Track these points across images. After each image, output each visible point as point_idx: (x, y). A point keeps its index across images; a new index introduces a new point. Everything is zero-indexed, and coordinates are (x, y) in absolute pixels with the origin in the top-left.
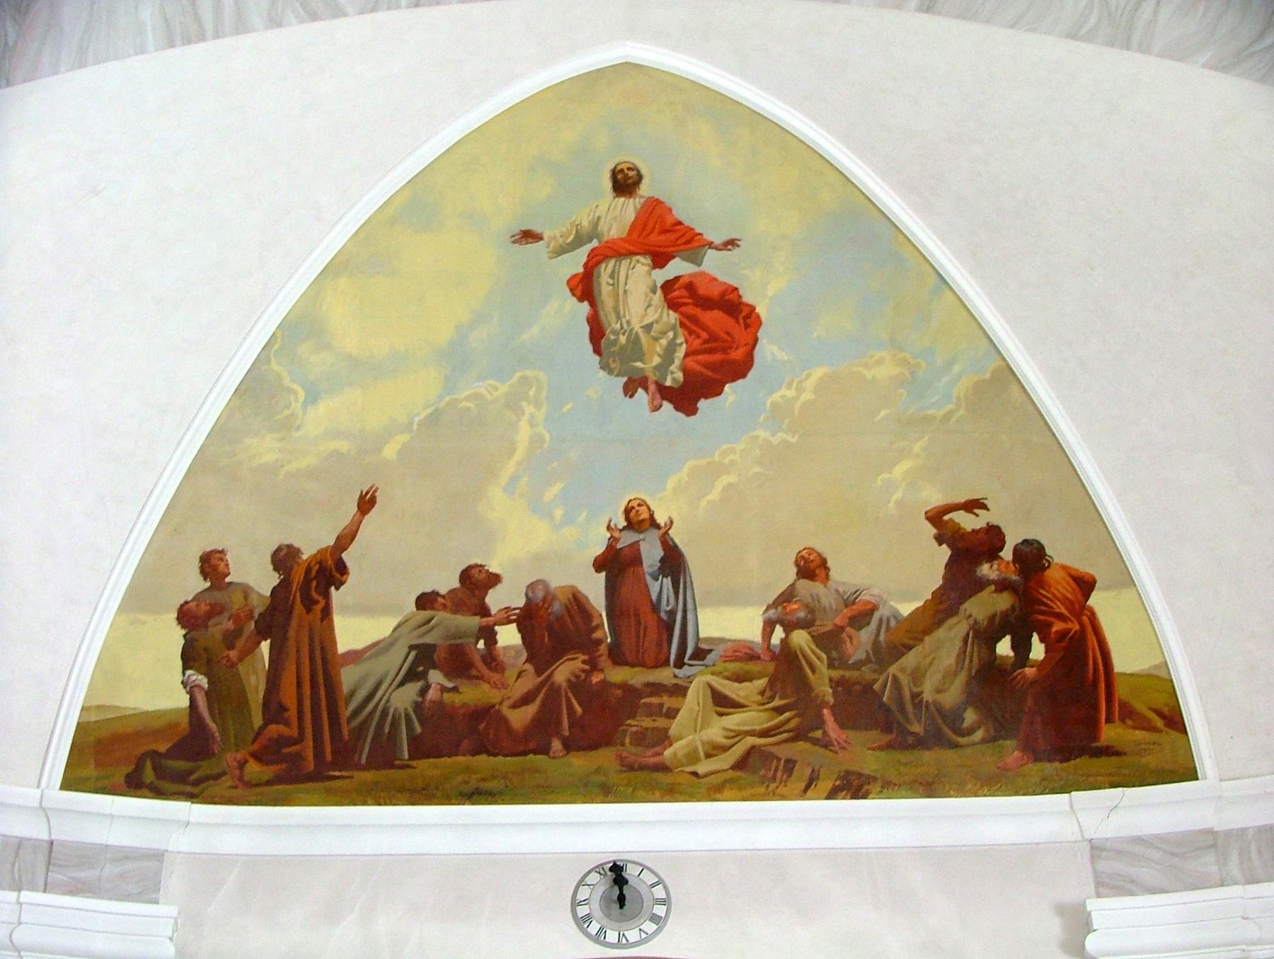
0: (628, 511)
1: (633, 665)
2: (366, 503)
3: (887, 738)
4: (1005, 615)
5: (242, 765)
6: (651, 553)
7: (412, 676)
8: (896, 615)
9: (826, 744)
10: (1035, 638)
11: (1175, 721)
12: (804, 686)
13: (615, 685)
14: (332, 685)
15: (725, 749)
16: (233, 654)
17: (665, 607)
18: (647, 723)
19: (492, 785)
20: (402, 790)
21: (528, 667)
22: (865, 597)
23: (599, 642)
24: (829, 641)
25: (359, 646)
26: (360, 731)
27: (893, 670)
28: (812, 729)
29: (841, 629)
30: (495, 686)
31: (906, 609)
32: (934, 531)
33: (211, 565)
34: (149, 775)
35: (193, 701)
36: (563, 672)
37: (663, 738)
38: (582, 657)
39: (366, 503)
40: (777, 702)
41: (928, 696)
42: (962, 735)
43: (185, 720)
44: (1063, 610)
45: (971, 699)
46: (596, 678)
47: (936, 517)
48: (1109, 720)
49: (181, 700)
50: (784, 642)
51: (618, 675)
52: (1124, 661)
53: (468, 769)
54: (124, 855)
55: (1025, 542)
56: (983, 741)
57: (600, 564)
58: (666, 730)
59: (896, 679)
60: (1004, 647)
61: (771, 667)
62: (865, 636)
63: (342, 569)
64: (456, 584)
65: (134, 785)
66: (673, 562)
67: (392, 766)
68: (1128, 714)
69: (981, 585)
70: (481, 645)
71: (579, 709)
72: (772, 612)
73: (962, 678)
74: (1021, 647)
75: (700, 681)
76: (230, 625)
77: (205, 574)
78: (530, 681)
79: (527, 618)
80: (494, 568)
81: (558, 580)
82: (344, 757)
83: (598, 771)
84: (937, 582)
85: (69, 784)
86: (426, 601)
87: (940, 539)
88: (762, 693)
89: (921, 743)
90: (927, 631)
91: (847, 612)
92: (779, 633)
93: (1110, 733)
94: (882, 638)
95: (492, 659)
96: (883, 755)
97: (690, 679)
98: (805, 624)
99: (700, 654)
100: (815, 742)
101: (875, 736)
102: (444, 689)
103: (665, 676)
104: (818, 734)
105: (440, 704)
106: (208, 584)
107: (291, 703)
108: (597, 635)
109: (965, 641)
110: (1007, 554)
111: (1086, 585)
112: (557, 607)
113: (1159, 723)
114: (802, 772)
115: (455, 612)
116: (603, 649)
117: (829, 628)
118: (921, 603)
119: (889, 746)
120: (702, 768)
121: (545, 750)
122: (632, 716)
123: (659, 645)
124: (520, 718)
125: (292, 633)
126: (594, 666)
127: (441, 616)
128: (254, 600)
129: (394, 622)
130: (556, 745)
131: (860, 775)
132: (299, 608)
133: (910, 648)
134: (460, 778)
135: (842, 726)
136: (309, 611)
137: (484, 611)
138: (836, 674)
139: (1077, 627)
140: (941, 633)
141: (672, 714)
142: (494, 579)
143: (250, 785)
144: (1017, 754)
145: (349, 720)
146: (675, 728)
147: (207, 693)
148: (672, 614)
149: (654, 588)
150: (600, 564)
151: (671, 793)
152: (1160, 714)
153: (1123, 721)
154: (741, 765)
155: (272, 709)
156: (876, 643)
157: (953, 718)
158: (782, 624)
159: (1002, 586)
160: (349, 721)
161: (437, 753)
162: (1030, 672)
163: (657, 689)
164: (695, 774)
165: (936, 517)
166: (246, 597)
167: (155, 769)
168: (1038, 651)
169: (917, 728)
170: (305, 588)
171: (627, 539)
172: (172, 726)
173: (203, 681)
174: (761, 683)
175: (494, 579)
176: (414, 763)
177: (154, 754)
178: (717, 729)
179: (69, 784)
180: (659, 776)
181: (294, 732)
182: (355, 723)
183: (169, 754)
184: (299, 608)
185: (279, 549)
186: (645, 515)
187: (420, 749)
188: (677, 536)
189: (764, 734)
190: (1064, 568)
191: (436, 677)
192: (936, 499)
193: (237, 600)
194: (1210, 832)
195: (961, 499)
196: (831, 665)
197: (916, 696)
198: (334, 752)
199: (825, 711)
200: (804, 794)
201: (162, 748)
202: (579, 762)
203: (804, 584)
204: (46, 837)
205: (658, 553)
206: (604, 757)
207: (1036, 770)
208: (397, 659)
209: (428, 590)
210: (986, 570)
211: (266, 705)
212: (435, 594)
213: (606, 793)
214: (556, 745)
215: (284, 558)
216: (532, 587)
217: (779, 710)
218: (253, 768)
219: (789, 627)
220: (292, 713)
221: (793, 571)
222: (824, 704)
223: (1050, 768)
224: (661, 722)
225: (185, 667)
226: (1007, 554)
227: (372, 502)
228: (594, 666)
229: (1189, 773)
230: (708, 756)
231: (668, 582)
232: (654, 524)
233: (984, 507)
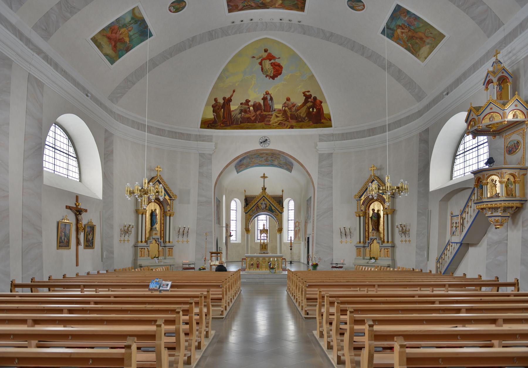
0: (266, 92)
1: (266, 112)
2: (234, 91)
3: (296, 121)
4: (311, 105)
5: (220, 124)
6: (269, 98)
7: (240, 113)
8: (298, 106)
9: (289, 122)
10: (315, 109)
11: (330, 120)
12: (287, 114)
13: (264, 114)
14: (231, 114)
15: (277, 122)
16: (219, 111)
17: (270, 105)
18: (268, 119)
19: (250, 127)
20: (239, 127)
21: (254, 112)
22: (295, 103)
23: (262, 109)
24: (290, 109)
25: (234, 109)
26: (234, 120)
27: (297, 112)
28: (288, 120)
29: (291, 107)
30: (250, 114)
31: (299, 105)
32: (303, 95)
33: (216, 100)
34: (210, 126)
35: (214, 117)
36: (258, 113)
37: (270, 121)
38: (260, 111)
39: (234, 91)
40: (283, 117)
41: (301, 115)
42: (305, 120)
43: (214, 120)
44: (318, 105)
45: (306, 116)
46: (262, 113)
47: (304, 93)
48: (323, 119)
49: (213, 117)
50: (284, 109)
51: (265, 113)
52: (325, 112)
53: (247, 125)
54: (208, 136)
55: (314, 97)
56: (308, 121)
57: (262, 99)
58: (270, 120)
59: (298, 114)
60: (311, 110)
61: (283, 112)
62: (294, 108)
63: (231, 100)
64: (245, 102)
65: (208, 127)
66: (271, 99)
67: (238, 124)
68: (325, 119)
69: (309, 102)
70: (248, 109)
71: (260, 117)
72: (283, 105)
73: (306, 113)
74: (313, 110)
75: (274, 114)
76: (218, 107)
77: (215, 101)
78: (254, 114)
79: (254, 106)
80: (250, 100)
81: (257, 101)
82: (232, 123)
83: (262, 125)
84: (304, 101)
85: (201, 128)
86: (241, 104)
87: (304, 96)
88: (282, 115)
89: (300, 122)
90: (302, 108)
91: (292, 105)
92: (284, 108)
93: (323, 121)
94: (296, 108)
95: (249, 111)
96: (296, 123)
97: (273, 114)
98: (287, 107)
99: (274, 110)
100: (288, 121)
101: (295, 121)
102: (244, 115)
103: (270, 113)
104: (288, 121)
105: (243, 117)
106: (215, 102)
107: (226, 116)
108: (262, 108)
109: (306, 109)
110: (312, 98)
111: (321, 102)
112: (257, 105)
113: (328, 120)
114: (286, 125)
115: (245, 105)
116: (263, 110)
117: (290, 107)
118: (301, 104)
119: (297, 122)
120: (274, 125)
121: (256, 123)
122: (266, 118)
123: (269, 109)
124: (253, 118)
125: (226, 108)
126: (262, 112)
127: (243, 106)
128: (221, 104)
129: (238, 107)
130: (257, 122)
131: (293, 126)
132: (226, 105)
133: (299, 110)
134: (246, 126)
135: (291, 119)
136: (227, 105)
137: (248, 105)
138: (291, 113)
139: (320, 107)
140: (303, 108)
141: (271, 118)
142: (250, 101)
143: (221, 127)
144: (312, 123)
145: (233, 119)
146: (271, 120)
147: (216, 116)
148: (271, 105)
149: (269, 102)
150: (262, 99)
151: (271, 128)
152: (329, 119)
153: (324, 119)
154: (279, 124)
155: (224, 117)
156: (296, 109)
157: (304, 118)
158: (284, 107)
159: (311, 102)
160: (233, 119)
161: (243, 123)
162: (314, 113)
163: (269, 115)
164: (273, 125)
165: (304, 93)
166: (220, 104)
167: (211, 125)
168: (315, 110)
169: (300, 120)
170: (227, 102)
171: (266, 96)
172: (212, 120)
173: (215, 114)
174: (282, 114)
175: (250, 101)
176: (241, 124)
177: (210, 123)
178: (276, 120)
179: (201, 128)
180: (269, 126)
181: (226, 120)
182: (234, 119)
183: (212, 123)
184: (226, 105)
185: (223, 98)
186: (268, 93)
187: (241, 123)
188: (272, 95)
189: (282, 120)
190: (319, 100)
191: (243, 113)
192: (304, 91)
193: (219, 104)
194: (333, 134)
195: (307, 91)
196: (290, 112)
197: (300, 116)
198: (231, 123)
199: (289, 118)
200: (286, 128)
201: (211, 122)
202: (260, 124)
203: (287, 101)
204: (199, 134)
205: (270, 98)
206: (263, 123)
207: (314, 124)
208: (238, 111)
209: (242, 102)
210: (310, 100)
211: (223, 117)
212: (243, 103)
213: (263, 128)
214: (257, 122)
215: (224, 99)
216: (254, 102)
217: (284, 117)
218: (222, 125)
219: (285, 107)
220: (226, 118)
221: (286, 100)
222: (289, 117)
223: (315, 125)
224: (270, 119)
225: (213, 113)
226: (312, 98)
227: (235, 91)
228: (262, 112)
229: (331, 126)
230: (275, 123)
231: (271, 101)
232: (269, 94)
233: (310, 92)
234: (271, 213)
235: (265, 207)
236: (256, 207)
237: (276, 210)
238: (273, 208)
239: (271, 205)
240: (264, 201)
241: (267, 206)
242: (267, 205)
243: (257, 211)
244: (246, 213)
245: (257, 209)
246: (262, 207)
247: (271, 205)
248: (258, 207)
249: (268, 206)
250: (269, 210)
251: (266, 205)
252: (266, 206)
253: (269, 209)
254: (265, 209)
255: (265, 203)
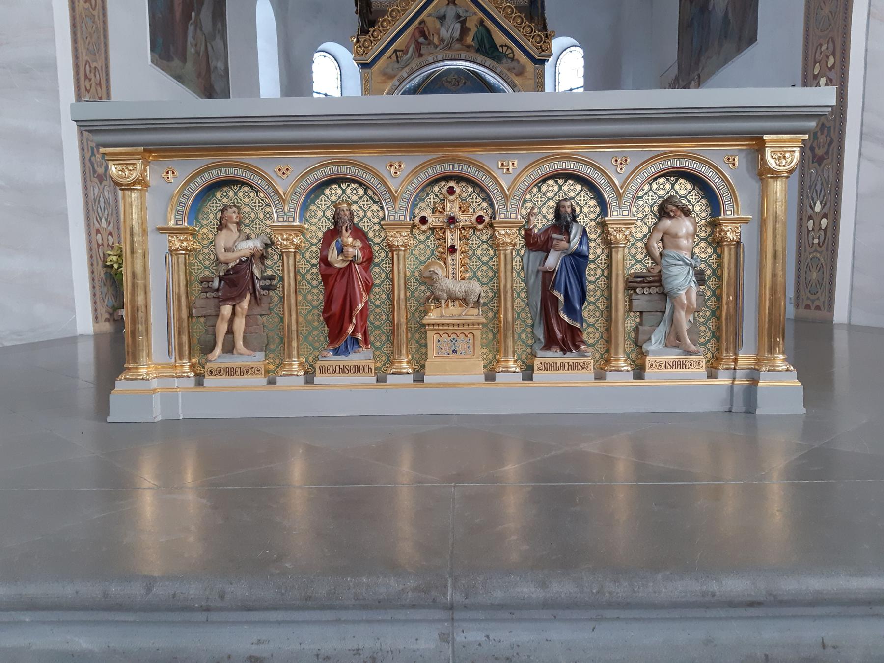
234: (489, 62)
235: (457, 34)
236: (413, 35)
237: (516, 49)
238: (500, 38)
239: (488, 23)
240: (451, 7)
241: (469, 29)
242: (468, 24)
243: (421, 55)
244: (364, 66)
245: (418, 46)
246: (445, 33)
247: (488, 23)
248: (426, 38)
249: (474, 30)
250: (478, 51)
251: (463, 23)
252: (464, 31)
253: (481, 43)
254: (458, 46)
255: (458, 16)
